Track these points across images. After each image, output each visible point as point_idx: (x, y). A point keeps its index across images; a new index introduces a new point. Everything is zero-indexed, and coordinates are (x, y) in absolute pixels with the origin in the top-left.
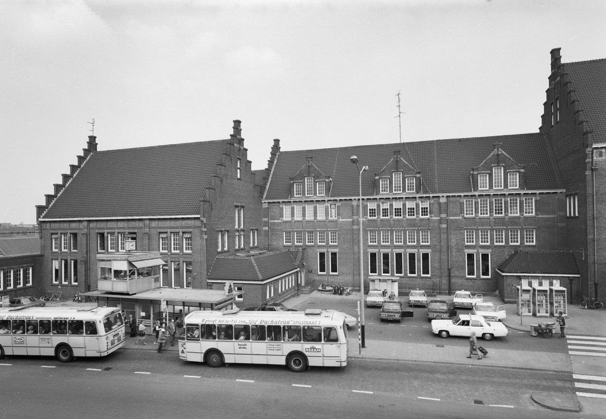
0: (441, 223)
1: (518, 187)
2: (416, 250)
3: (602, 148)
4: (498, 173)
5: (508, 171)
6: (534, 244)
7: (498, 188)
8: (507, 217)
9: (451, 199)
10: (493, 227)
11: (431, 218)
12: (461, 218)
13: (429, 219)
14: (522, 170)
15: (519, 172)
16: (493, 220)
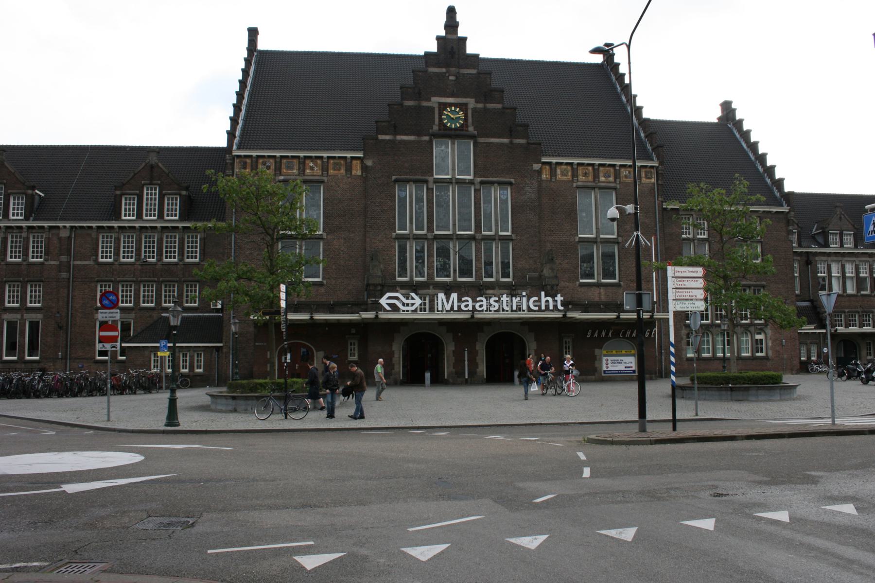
0: (60, 272)
1: (177, 218)
2: (19, 316)
3: (246, 156)
4: (151, 195)
5: (164, 192)
6: (196, 305)
7: (150, 219)
8: (159, 263)
9: (79, 231)
10: (139, 279)
11: (46, 263)
12: (91, 263)
13: (42, 264)
14: (184, 193)
15: (181, 195)
16: (140, 267)
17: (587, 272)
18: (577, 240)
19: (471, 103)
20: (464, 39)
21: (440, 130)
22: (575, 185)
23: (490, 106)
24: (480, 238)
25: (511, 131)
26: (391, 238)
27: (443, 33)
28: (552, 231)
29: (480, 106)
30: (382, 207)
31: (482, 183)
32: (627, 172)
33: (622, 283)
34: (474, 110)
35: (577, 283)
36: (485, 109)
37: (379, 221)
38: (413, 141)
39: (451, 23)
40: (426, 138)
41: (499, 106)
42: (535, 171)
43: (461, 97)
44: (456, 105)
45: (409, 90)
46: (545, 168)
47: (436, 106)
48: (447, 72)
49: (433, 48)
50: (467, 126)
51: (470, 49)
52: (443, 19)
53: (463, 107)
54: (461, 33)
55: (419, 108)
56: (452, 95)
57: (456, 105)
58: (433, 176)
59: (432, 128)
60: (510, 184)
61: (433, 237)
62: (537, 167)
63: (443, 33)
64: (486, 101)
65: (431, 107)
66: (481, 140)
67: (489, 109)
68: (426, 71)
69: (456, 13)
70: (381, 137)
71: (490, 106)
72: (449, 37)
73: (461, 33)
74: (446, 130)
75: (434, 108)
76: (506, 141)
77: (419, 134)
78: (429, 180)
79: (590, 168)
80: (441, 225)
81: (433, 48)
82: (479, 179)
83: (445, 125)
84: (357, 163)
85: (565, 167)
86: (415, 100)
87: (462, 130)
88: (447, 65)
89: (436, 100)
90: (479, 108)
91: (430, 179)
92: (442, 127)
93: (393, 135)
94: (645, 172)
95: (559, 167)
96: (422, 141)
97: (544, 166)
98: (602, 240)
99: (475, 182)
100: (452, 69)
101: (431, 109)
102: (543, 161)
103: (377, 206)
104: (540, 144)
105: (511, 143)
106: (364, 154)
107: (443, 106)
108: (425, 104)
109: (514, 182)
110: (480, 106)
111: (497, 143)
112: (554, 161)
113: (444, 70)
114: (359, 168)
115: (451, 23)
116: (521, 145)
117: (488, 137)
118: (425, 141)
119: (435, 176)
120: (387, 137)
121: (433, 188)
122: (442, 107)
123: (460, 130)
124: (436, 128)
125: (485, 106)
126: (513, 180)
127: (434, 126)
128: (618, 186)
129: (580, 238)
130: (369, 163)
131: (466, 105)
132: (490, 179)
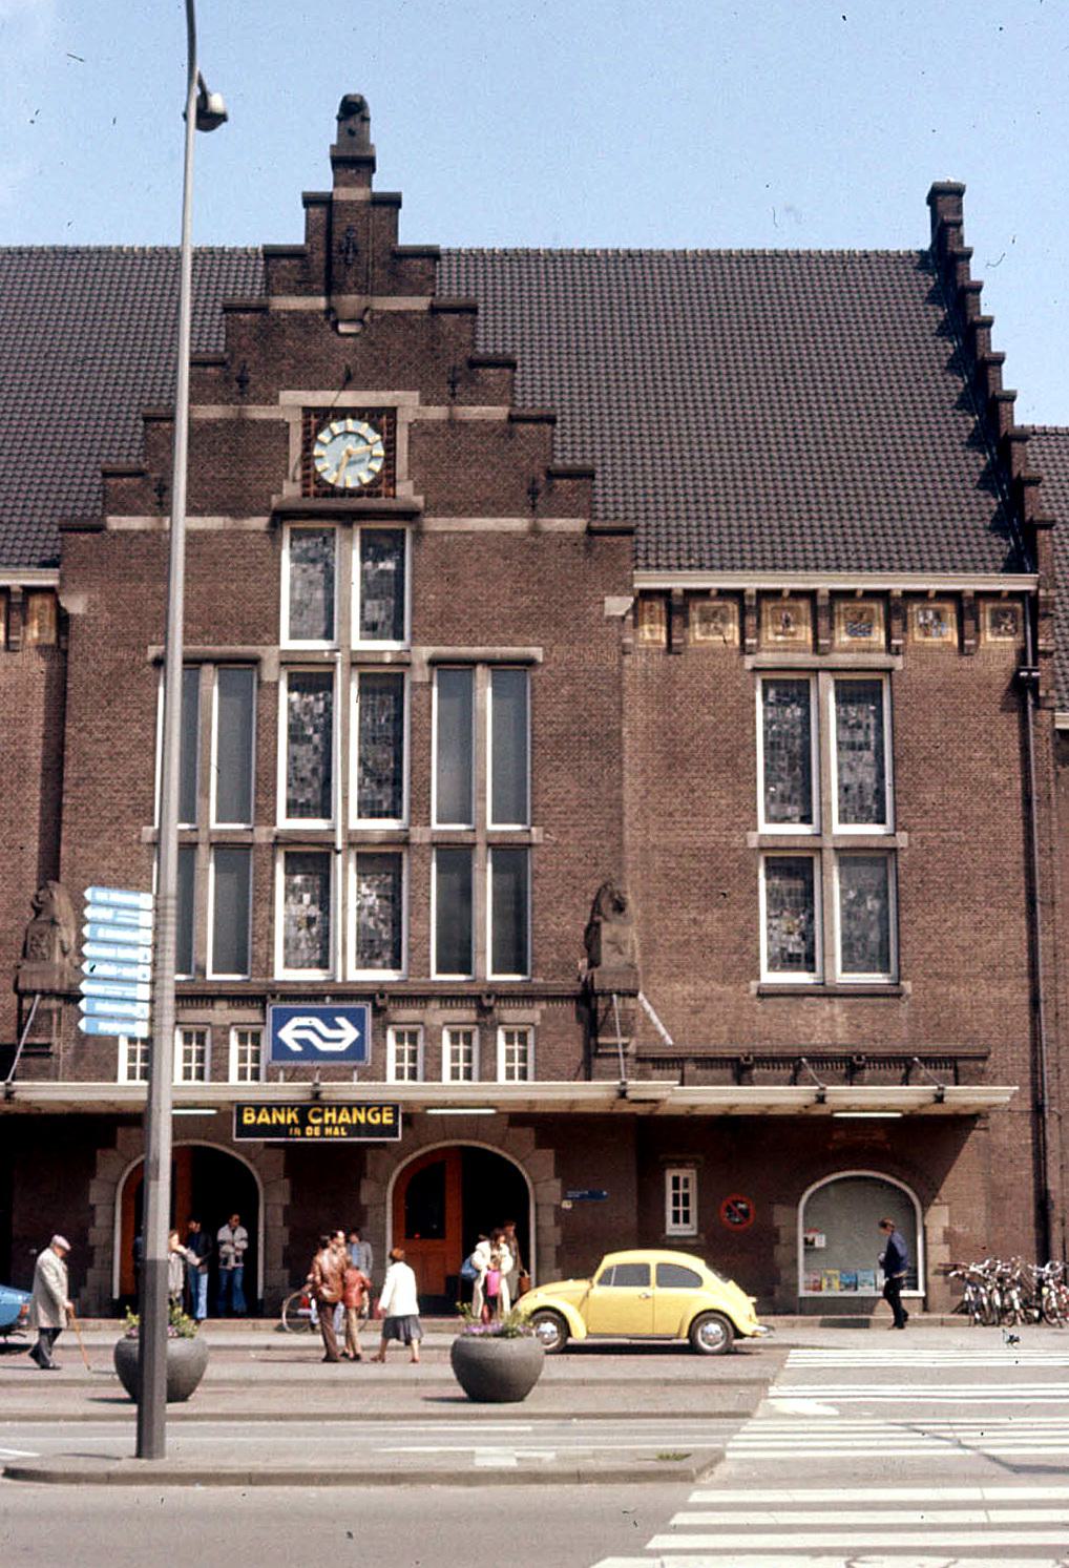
17: (790, 950)
18: (753, 844)
19: (408, 404)
20: (393, 202)
21: (305, 495)
22: (749, 662)
23: (472, 413)
24: (426, 840)
25: (533, 492)
26: (139, 842)
27: (323, 181)
28: (671, 815)
29: (437, 413)
30: (114, 746)
31: (433, 662)
32: (931, 615)
33: (907, 986)
34: (419, 429)
35: (754, 984)
36: (452, 422)
37: (99, 789)
38: (219, 533)
39: (353, 160)
40: (260, 523)
41: (500, 412)
42: (610, 619)
43: (377, 389)
44: (357, 413)
45: (210, 370)
46: (651, 609)
47: (295, 419)
48: (330, 310)
49: (291, 230)
50: (393, 484)
51: (412, 232)
52: (328, 132)
53: (382, 419)
54: (382, 182)
55: (241, 424)
56: (347, 382)
57: (357, 413)
58: (278, 643)
59: (280, 492)
60: (530, 663)
61: (271, 840)
62: (618, 605)
63: (323, 181)
64: (453, 399)
65: (277, 422)
66: (435, 524)
67: (464, 424)
68: (263, 309)
69: (366, 119)
70: (115, 523)
71: (472, 413)
72: (344, 194)
73: (381, 183)
74: (325, 495)
75: (288, 425)
76: (518, 524)
77: (237, 510)
78: (265, 657)
79: (803, 605)
80: (301, 800)
81: (291, 230)
82: (425, 652)
83: (320, 482)
84: (43, 607)
85: (720, 604)
86: (226, 403)
87: (378, 494)
88: (330, 288)
89: (293, 401)
90: (433, 422)
91: (270, 655)
92: (313, 488)
93: (155, 515)
94: (995, 612)
95: (698, 605)
96: (247, 532)
97: (647, 604)
98: (840, 845)
99: (415, 661)
100: (350, 302)
101: (280, 429)
102: (638, 585)
103: (98, 741)
104: (629, 532)
105: (535, 531)
106: (61, 578)
107: (318, 418)
108: (258, 412)
109: (540, 659)
110: (437, 413)
111: (487, 533)
112: (679, 582)
113: (321, 302)
114: (47, 623)
115: (353, 160)
116: (565, 538)
117: (459, 514)
118: (255, 532)
119: (287, 643)
120: (136, 523)
121: (277, 684)
122: (314, 420)
123: (369, 495)
124: (291, 491)
125: (451, 412)
126: (537, 653)
127: (285, 484)
128: (898, 663)
129: (762, 836)
130: (75, 605)
131: (391, 412)
132: (464, 651)
